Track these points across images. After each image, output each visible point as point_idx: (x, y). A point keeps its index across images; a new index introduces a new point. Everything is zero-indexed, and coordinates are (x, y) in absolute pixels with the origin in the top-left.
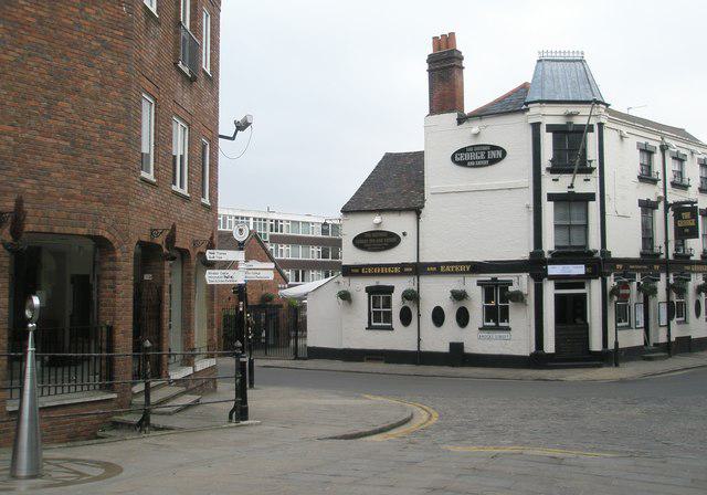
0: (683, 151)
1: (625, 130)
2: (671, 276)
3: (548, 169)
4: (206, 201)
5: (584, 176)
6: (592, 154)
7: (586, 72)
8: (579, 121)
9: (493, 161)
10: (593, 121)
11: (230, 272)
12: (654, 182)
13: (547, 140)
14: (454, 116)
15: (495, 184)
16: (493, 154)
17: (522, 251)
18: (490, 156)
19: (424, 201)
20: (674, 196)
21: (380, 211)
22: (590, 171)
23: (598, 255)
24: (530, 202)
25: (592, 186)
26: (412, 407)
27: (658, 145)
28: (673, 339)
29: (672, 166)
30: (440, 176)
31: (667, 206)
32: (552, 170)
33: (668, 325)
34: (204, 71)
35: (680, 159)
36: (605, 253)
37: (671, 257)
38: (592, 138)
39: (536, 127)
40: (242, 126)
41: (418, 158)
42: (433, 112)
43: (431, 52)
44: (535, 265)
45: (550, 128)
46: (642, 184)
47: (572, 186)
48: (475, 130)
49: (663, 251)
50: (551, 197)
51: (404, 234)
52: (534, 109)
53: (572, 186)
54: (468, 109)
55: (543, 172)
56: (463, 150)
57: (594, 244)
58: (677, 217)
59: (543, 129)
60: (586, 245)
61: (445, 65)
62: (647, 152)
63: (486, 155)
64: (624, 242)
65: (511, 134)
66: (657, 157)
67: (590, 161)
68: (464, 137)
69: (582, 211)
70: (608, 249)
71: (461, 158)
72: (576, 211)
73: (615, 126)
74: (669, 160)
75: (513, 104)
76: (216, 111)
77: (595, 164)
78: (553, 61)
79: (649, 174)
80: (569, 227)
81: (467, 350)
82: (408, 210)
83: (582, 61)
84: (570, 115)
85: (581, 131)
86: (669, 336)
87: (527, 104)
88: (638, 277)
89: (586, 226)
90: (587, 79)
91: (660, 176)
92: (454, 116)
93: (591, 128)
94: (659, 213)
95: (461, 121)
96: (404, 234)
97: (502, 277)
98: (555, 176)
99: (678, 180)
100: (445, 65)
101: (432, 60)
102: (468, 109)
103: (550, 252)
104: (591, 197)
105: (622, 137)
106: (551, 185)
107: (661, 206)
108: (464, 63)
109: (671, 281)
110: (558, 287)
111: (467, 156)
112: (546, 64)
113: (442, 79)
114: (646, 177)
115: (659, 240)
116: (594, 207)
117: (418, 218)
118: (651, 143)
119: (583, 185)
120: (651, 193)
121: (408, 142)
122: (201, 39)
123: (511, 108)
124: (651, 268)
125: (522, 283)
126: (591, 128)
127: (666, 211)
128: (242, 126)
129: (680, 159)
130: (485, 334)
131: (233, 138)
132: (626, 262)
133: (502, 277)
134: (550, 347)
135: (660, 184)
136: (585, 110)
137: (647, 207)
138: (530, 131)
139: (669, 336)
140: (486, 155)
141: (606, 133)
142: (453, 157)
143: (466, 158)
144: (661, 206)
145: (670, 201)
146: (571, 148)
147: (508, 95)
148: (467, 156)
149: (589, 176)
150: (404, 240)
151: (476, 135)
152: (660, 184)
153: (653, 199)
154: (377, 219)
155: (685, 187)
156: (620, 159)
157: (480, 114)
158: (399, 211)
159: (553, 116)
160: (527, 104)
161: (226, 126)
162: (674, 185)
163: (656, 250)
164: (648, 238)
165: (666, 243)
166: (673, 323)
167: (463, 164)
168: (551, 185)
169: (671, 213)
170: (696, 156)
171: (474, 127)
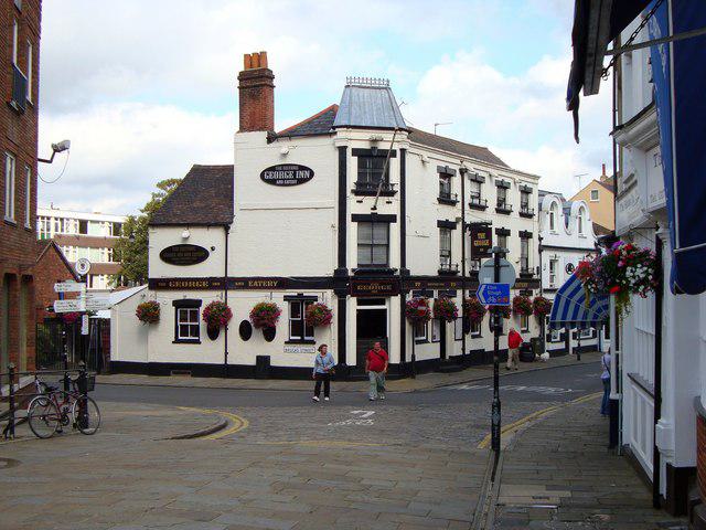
0: (481, 174)
1: (426, 155)
2: (467, 292)
3: (353, 191)
4: (28, 225)
5: (386, 199)
6: (395, 178)
7: (391, 100)
8: (383, 146)
9: (302, 181)
10: (396, 147)
11: (74, 302)
12: (453, 203)
13: (352, 163)
14: (264, 134)
15: (304, 203)
16: (301, 174)
17: (327, 269)
18: (298, 175)
19: (232, 216)
20: (473, 217)
21: (188, 225)
22: (392, 194)
23: (398, 273)
24: (336, 222)
25: (392, 208)
26: (226, 415)
27: (457, 168)
28: (467, 352)
29: (470, 188)
30: (248, 191)
31: (465, 226)
32: (356, 193)
33: (463, 339)
34: (28, 102)
35: (478, 181)
36: (405, 271)
37: (467, 275)
38: (395, 163)
39: (342, 150)
40: (57, 149)
41: (227, 172)
42: (242, 129)
43: (243, 69)
44: (340, 282)
45: (355, 152)
46: (441, 206)
47: (375, 208)
48: (284, 150)
49: (460, 268)
50: (355, 218)
51: (213, 249)
52: (341, 133)
53: (375, 208)
54: (279, 128)
55: (349, 193)
56: (272, 169)
57: (395, 263)
58: (474, 237)
59: (349, 152)
60: (387, 265)
61: (256, 83)
62: (446, 175)
63: (294, 175)
64: (424, 260)
65: (318, 155)
66: (456, 181)
67: (393, 185)
68: (273, 155)
69: (384, 232)
70: (408, 267)
71: (270, 176)
72: (379, 231)
73: (416, 151)
74: (467, 182)
75: (321, 126)
76: (36, 136)
77: (397, 188)
78: (359, 87)
79: (449, 195)
80: (372, 246)
81: (273, 363)
82: (217, 225)
83: (387, 88)
84: (374, 141)
85: (386, 155)
86: (463, 349)
87: (334, 128)
88: (436, 293)
89: (388, 246)
90: (393, 108)
91: (459, 198)
92: (264, 134)
93: (393, 154)
94: (457, 234)
95: (271, 139)
96: (213, 249)
97: (308, 293)
98: (360, 198)
99: (476, 201)
100: (256, 83)
101: (243, 77)
102: (279, 128)
103: (353, 270)
104: (392, 218)
105: (423, 162)
106: (357, 206)
107: (459, 226)
108: (275, 82)
109: (467, 297)
110: (359, 303)
111: (276, 175)
112: (354, 90)
113: (253, 97)
114: (445, 199)
115: (456, 258)
116: (395, 228)
117: (227, 234)
118: (451, 166)
119: (388, 207)
120: (450, 214)
121: (218, 154)
122: (27, 76)
123: (319, 130)
124: (449, 286)
125: (328, 298)
126: (393, 154)
127: (464, 232)
128: (57, 149)
129: (478, 181)
130: (290, 347)
131: (50, 162)
132: (425, 280)
133: (308, 293)
134: (351, 360)
135: (459, 205)
136: (388, 136)
137: (445, 226)
138: (337, 153)
139: (463, 349)
140: (294, 175)
141: (408, 157)
142: (262, 175)
143: (278, 176)
144: (459, 226)
145: (468, 220)
146: (374, 170)
147: (317, 117)
148: (276, 175)
149: (390, 199)
150: (212, 256)
151: (285, 155)
152: (459, 205)
153: (453, 220)
154: (185, 233)
155: (483, 208)
156: (420, 178)
157: (291, 134)
158: (208, 225)
159: (360, 140)
160: (334, 128)
161: (44, 150)
162: (472, 206)
163: (453, 268)
164: (446, 254)
165: (463, 261)
166: (468, 337)
167: (272, 182)
168: (357, 206)
169: (468, 233)
170: (494, 179)
171: (283, 146)
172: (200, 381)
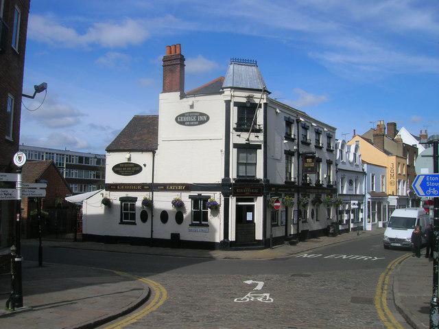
0: (307, 124)
3: (234, 129)
4: (10, 138)
11: (10, 191)
17: (218, 178)
18: (197, 119)
19: (157, 145)
20: (303, 150)
26: (150, 282)
27: (295, 119)
28: (300, 232)
30: (167, 129)
31: (299, 155)
32: (236, 130)
33: (298, 224)
39: (228, 103)
40: (40, 89)
44: (225, 187)
45: (236, 104)
50: (236, 146)
52: (228, 92)
53: (248, 140)
54: (186, 91)
56: (183, 115)
59: (232, 104)
63: (197, 119)
67: (259, 125)
68: (184, 106)
74: (300, 128)
81: (182, 238)
82: (150, 151)
91: (296, 137)
94: (294, 159)
95: (182, 96)
97: (204, 194)
98: (239, 133)
103: (234, 179)
104: (259, 147)
106: (236, 138)
110: (238, 200)
111: (185, 119)
116: (260, 153)
118: (292, 118)
125: (217, 197)
128: (40, 89)
130: (193, 228)
131: (33, 97)
133: (204, 194)
134: (232, 237)
137: (289, 154)
139: (298, 230)
140: (197, 119)
141: (268, 109)
143: (183, 120)
144: (296, 154)
152: (296, 141)
154: (127, 155)
158: (142, 151)
160: (223, 89)
161: (28, 88)
162: (303, 142)
166: (300, 222)
167: (182, 123)
168: (236, 138)
169: (301, 159)
171: (190, 101)
172: (134, 249)
